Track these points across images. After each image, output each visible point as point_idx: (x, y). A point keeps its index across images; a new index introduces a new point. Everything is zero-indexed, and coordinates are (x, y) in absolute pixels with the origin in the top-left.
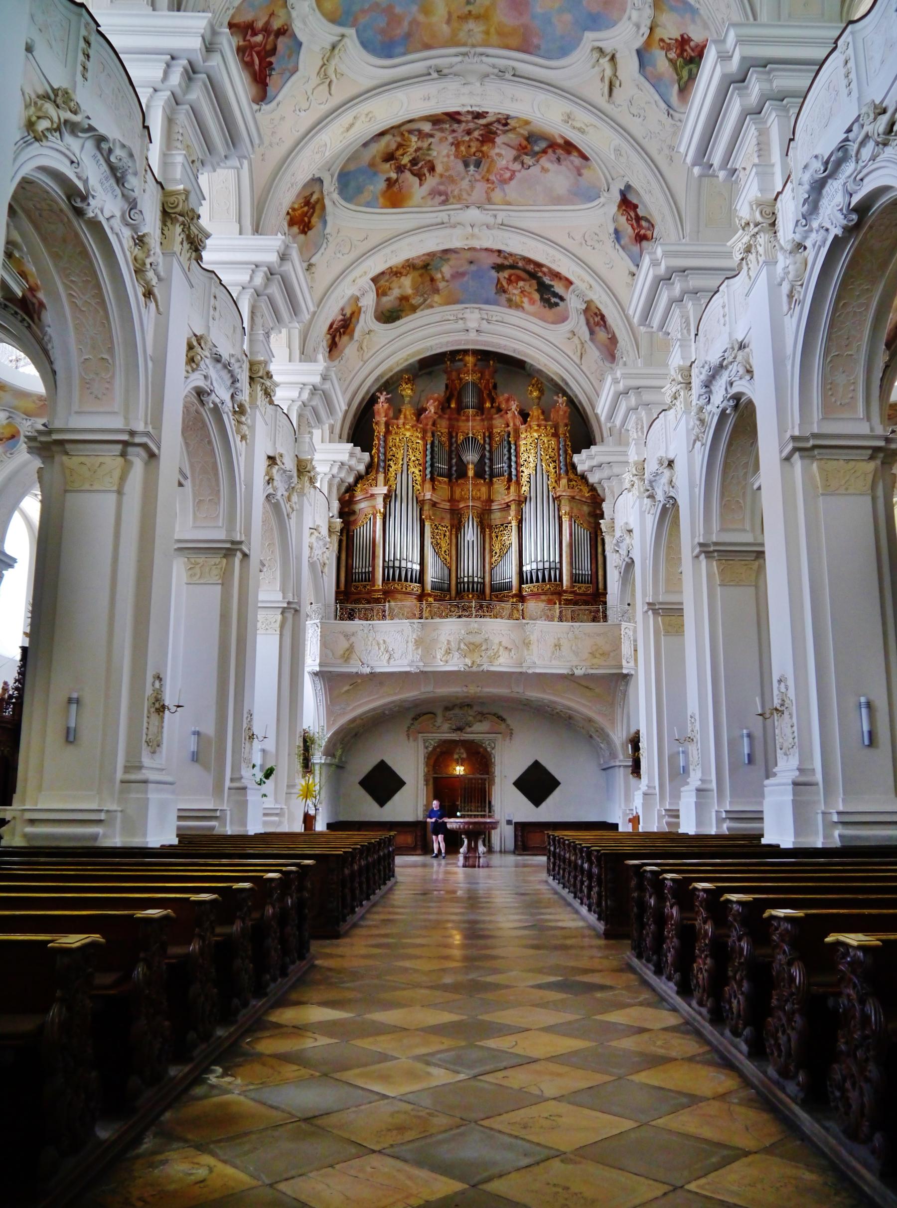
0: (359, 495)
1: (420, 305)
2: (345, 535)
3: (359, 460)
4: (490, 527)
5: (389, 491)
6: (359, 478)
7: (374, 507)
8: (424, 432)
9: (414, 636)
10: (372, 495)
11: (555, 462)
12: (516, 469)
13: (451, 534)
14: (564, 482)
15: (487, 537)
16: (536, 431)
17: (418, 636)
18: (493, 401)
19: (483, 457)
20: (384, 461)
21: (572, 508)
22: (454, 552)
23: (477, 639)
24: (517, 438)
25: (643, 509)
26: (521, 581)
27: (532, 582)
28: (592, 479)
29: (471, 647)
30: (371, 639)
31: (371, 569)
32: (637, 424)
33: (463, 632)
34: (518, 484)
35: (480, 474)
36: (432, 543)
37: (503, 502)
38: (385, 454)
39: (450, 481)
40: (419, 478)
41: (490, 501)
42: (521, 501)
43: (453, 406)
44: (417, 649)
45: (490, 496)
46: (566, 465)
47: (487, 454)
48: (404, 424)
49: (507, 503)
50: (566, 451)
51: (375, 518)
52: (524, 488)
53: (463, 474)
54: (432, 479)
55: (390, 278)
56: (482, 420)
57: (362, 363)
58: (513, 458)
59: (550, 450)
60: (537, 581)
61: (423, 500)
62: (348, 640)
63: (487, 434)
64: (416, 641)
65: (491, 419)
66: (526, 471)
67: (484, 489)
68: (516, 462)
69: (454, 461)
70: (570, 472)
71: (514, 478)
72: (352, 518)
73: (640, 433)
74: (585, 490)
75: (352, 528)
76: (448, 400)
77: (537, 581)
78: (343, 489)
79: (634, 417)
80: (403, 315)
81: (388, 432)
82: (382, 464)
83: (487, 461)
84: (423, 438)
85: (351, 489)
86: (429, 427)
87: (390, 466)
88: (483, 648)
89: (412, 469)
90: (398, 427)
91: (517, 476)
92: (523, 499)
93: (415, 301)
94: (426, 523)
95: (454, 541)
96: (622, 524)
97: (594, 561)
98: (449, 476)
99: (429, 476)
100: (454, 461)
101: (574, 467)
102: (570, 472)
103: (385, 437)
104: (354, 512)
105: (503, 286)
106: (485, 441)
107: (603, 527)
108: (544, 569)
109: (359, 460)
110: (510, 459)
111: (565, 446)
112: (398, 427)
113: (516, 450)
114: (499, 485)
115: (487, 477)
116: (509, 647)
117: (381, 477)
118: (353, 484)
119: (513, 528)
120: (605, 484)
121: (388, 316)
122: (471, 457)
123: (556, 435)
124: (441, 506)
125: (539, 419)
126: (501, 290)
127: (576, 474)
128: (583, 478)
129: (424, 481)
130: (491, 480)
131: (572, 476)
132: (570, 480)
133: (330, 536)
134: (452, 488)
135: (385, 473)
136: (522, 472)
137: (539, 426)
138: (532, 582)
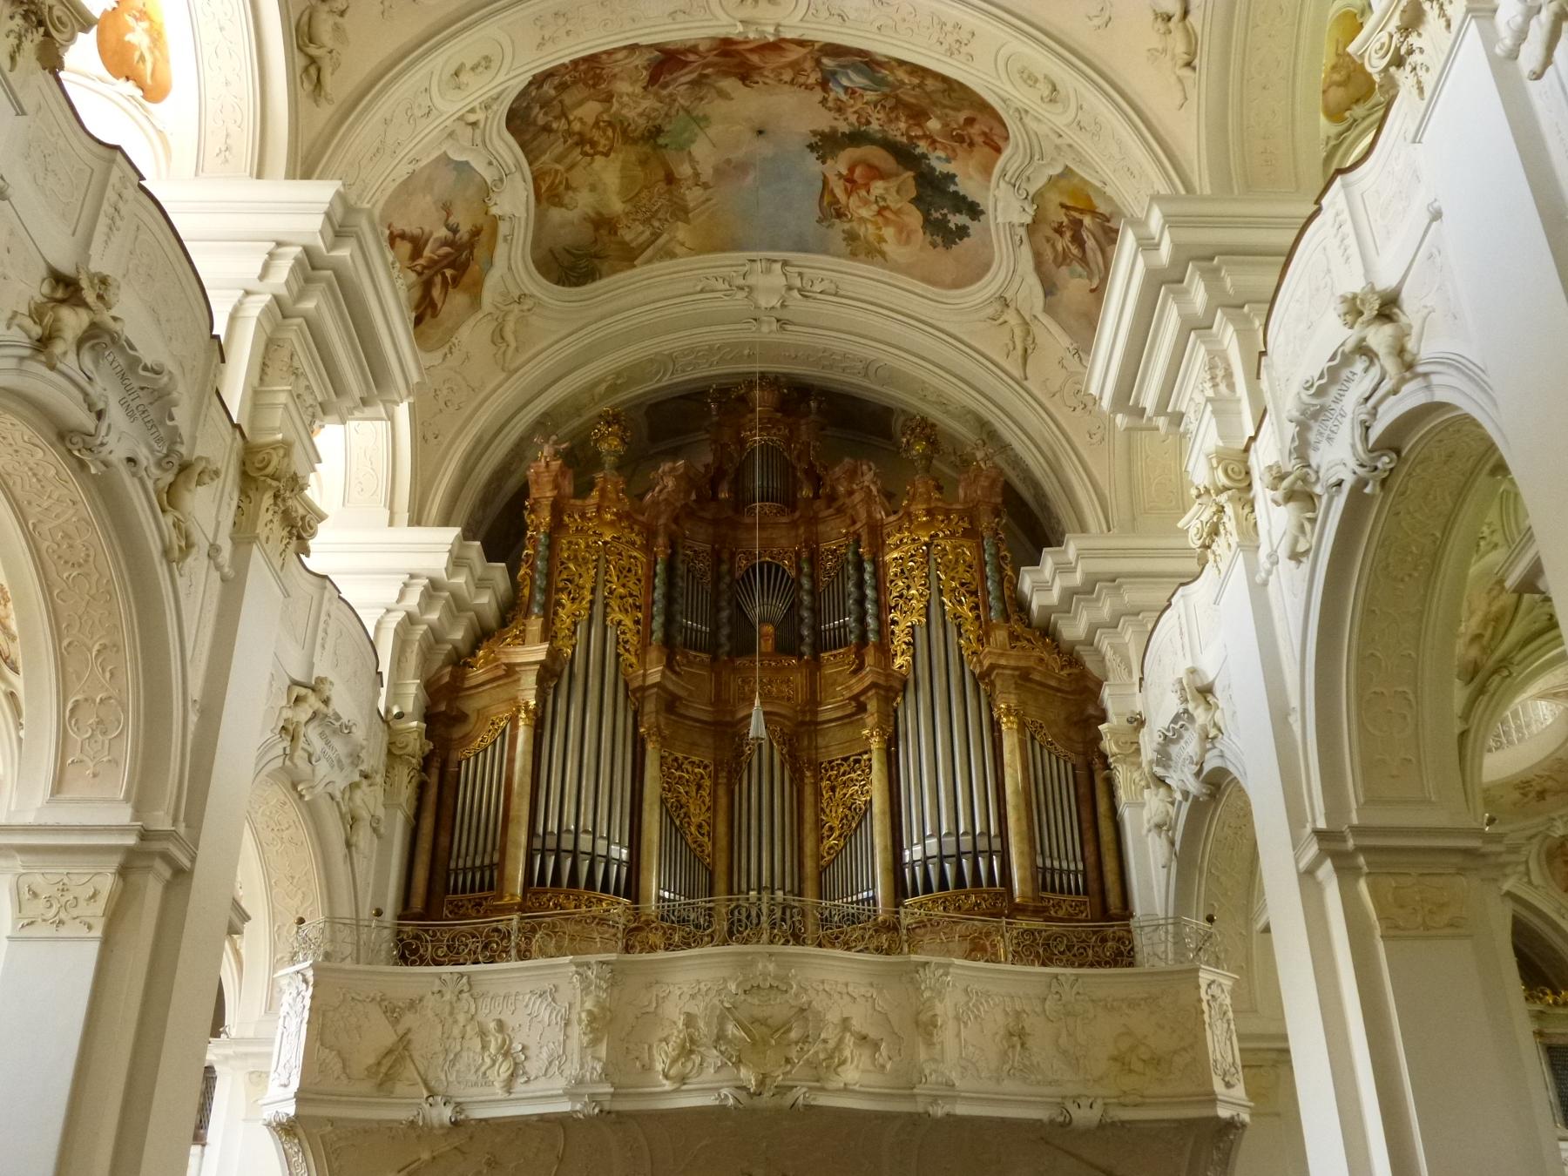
0: (478, 674)
1: (643, 248)
2: (435, 773)
3: (484, 589)
4: (817, 768)
5: (553, 654)
6: (482, 636)
7: (514, 699)
8: (650, 533)
9: (589, 1005)
10: (511, 670)
11: (974, 593)
12: (878, 617)
13: (716, 784)
14: (1000, 635)
15: (808, 792)
16: (923, 525)
17: (598, 1003)
18: (817, 482)
19: (794, 607)
20: (547, 591)
21: (1022, 703)
22: (722, 828)
23: (777, 1009)
24: (878, 547)
25: (1258, 579)
26: (900, 890)
27: (928, 888)
28: (1073, 629)
29: (757, 1031)
30: (461, 1018)
31: (496, 858)
32: (1212, 368)
33: (733, 987)
34: (885, 653)
35: (787, 645)
36: (663, 801)
37: (847, 694)
38: (549, 575)
39: (715, 659)
40: (634, 640)
41: (813, 702)
42: (893, 690)
43: (723, 495)
44: (595, 1042)
45: (813, 692)
46: (1001, 598)
47: (806, 598)
48: (599, 509)
49: (855, 698)
50: (999, 570)
51: (515, 727)
52: (899, 661)
53: (745, 647)
54: (668, 642)
55: (569, 150)
56: (794, 525)
57: (503, 375)
58: (869, 592)
59: (961, 569)
60: (943, 885)
61: (643, 688)
62: (396, 1022)
63: (804, 555)
64: (592, 1017)
65: (814, 520)
66: (903, 623)
67: (799, 679)
68: (877, 602)
69: (725, 614)
70: (1014, 617)
71: (872, 637)
72: (457, 733)
73: (1223, 388)
74: (1054, 661)
75: (457, 755)
76: (714, 484)
77: (943, 885)
78: (439, 659)
79: (1203, 350)
80: (605, 267)
81: (557, 526)
82: (539, 597)
83: (806, 614)
84: (647, 548)
85: (460, 661)
86: (662, 521)
87: (559, 603)
88: (793, 1035)
89: (619, 616)
90: (583, 516)
91: (879, 632)
92: (897, 685)
93: (632, 234)
94: (650, 747)
95: (723, 801)
96: (1181, 673)
97: (1089, 835)
98: (712, 647)
99: (658, 635)
100: (725, 614)
101: (1022, 606)
102: (1014, 617)
103: (549, 535)
104: (462, 718)
105: (835, 201)
106: (799, 570)
107: (1108, 745)
108: (959, 856)
109: (484, 589)
110: (861, 601)
111: (997, 556)
112: (583, 516)
113: (875, 574)
114: (835, 664)
115: (805, 649)
116: (873, 1034)
117: (535, 625)
118: (464, 648)
119: (875, 765)
120: (1105, 643)
121: (571, 264)
122: (763, 609)
123: (971, 533)
124: (692, 713)
125: (929, 499)
126: (833, 211)
127: (1029, 625)
128: (1047, 632)
129: (645, 645)
130: (816, 657)
131: (1018, 628)
132: (1014, 637)
133: (389, 769)
134: (718, 675)
135: (546, 616)
136: (894, 622)
137: (929, 512)
138: (928, 888)
